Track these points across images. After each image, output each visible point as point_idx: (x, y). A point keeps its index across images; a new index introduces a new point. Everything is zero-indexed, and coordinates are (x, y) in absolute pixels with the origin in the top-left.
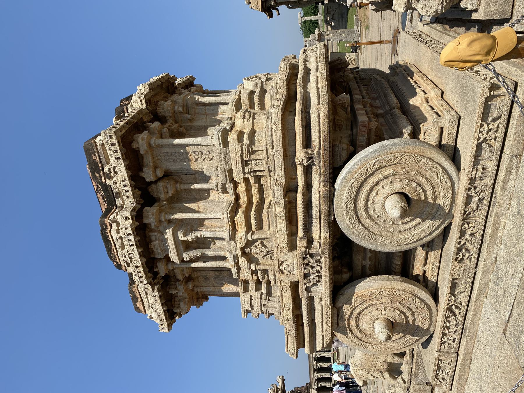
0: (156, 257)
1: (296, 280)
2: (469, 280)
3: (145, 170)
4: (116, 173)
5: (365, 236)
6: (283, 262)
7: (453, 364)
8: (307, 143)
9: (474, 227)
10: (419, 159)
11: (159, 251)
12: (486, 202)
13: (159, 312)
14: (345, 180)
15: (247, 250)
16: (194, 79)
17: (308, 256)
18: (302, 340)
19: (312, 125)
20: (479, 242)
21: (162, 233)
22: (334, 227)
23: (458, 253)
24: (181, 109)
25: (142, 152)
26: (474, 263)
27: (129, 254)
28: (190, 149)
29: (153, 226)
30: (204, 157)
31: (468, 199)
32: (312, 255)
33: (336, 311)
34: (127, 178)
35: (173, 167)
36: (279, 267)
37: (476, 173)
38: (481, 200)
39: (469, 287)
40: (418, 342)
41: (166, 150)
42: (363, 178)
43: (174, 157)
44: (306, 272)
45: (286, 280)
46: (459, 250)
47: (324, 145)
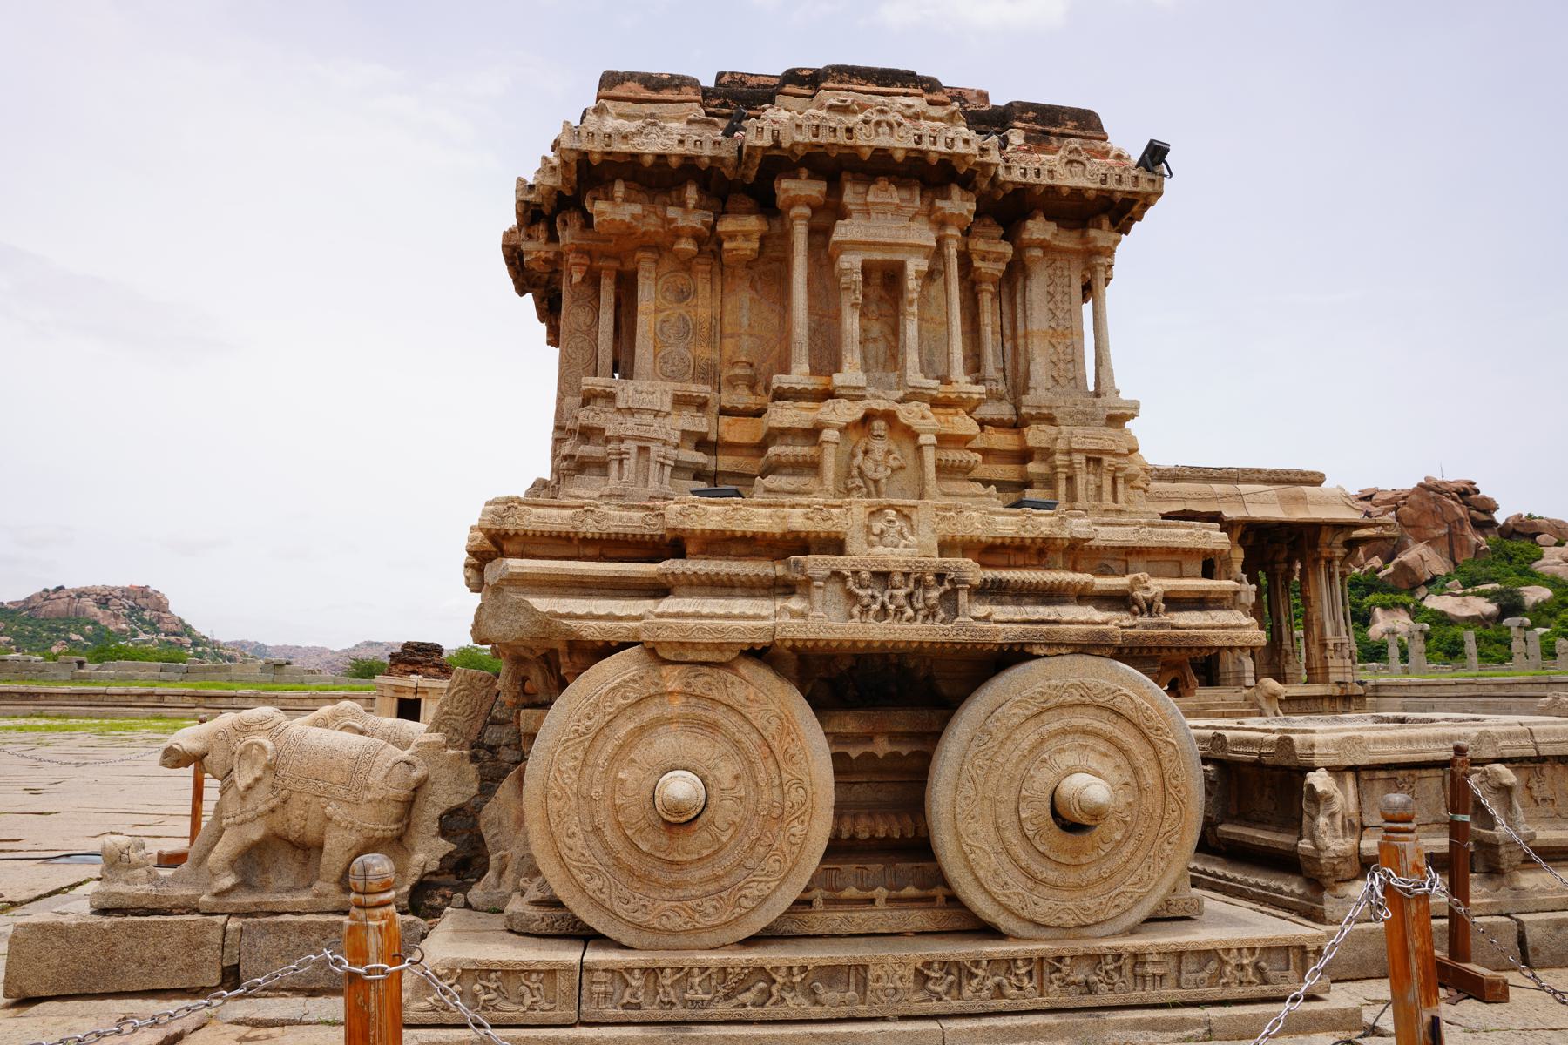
2: (862, 1010)
4: (1070, 162)
5: (990, 733)
6: (907, 517)
7: (537, 1015)
8: (1175, 602)
9: (1020, 988)
10: (1173, 839)
11: (870, 198)
12: (1089, 1001)
13: (636, 140)
14: (1135, 685)
15: (879, 426)
17: (947, 586)
18: (539, 552)
20: (981, 1010)
22: (1011, 656)
26: (918, 1009)
27: (890, 125)
29: (939, 203)
30: (1062, 366)
33: (729, 656)
36: (890, 506)
37: (1154, 963)
38: (1089, 988)
39: (843, 1011)
42: (1142, 719)
43: (1058, 297)
44: (897, 578)
45: (849, 518)
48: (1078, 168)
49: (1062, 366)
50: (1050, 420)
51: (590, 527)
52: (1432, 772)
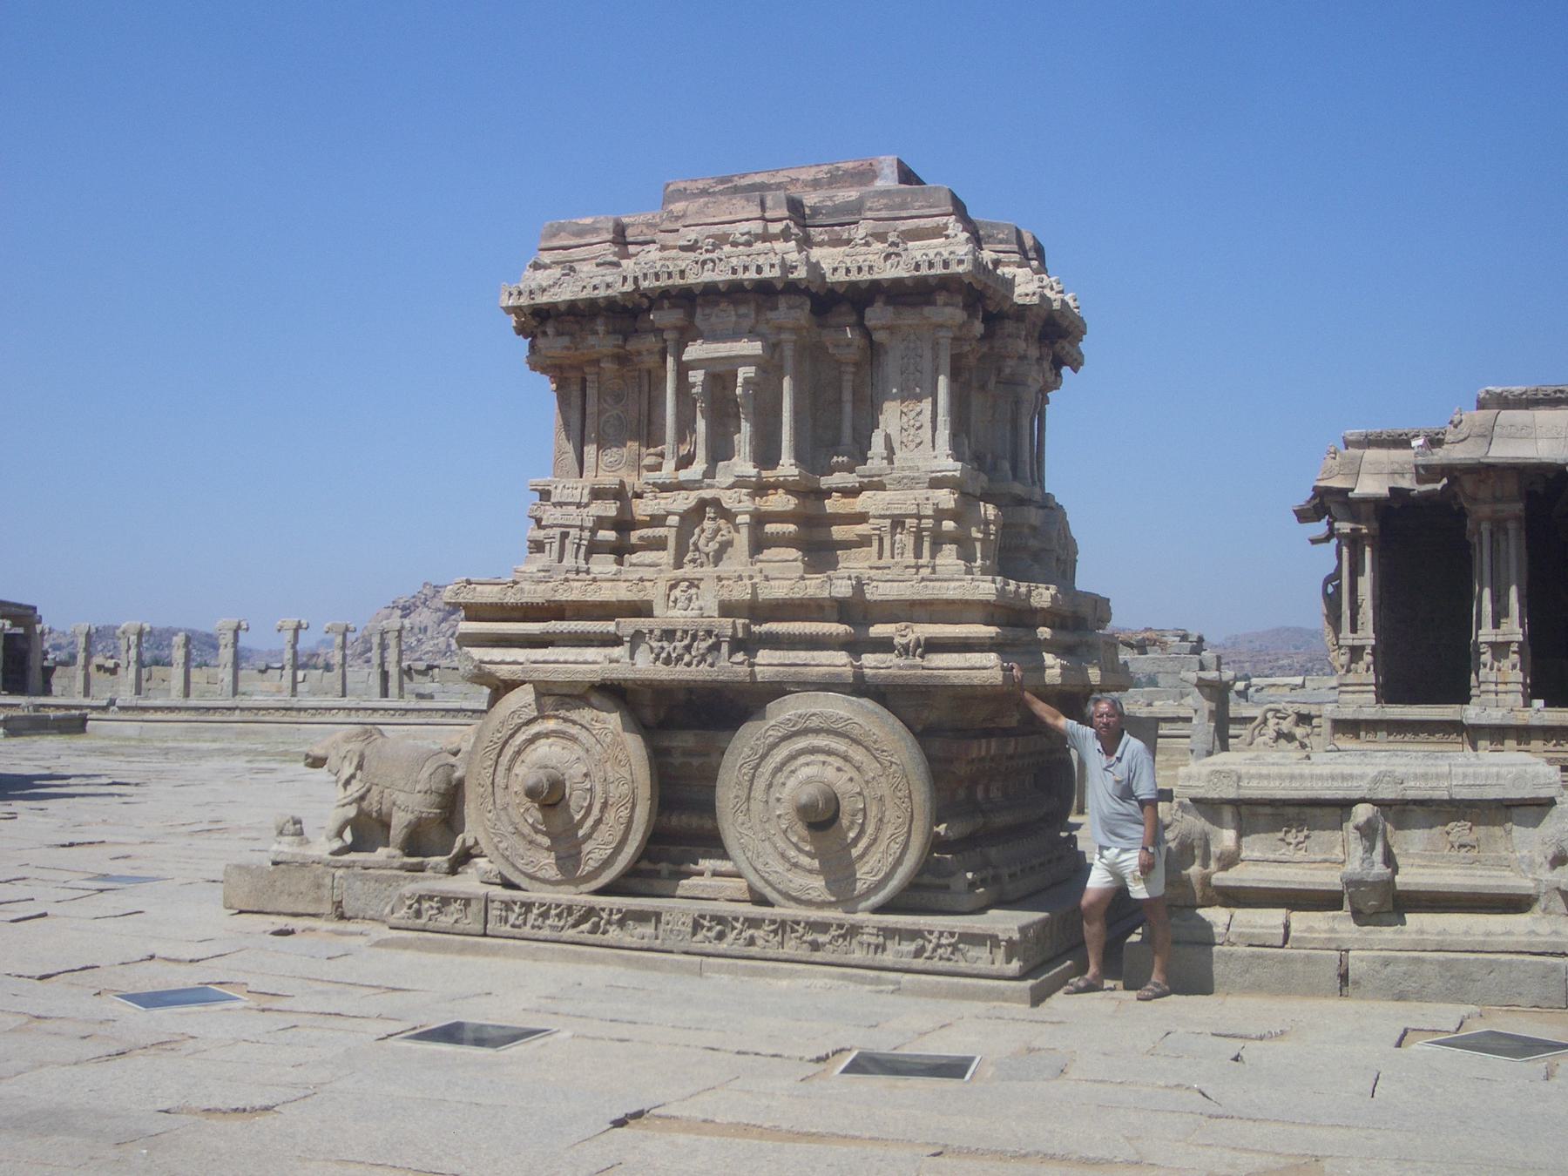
0: (699, 310)
1: (656, 613)
2: (657, 944)
3: (890, 308)
4: (888, 257)
8: (934, 646)
12: (818, 956)
13: (555, 290)
15: (710, 512)
16: (1075, 370)
19: (968, 655)
21: (753, 334)
23: (713, 918)
24: (1008, 371)
25: (927, 310)
28: (926, 405)
31: (823, 927)
32: (716, 647)
34: (876, 276)
35: (892, 365)
36: (685, 580)
39: (645, 943)
40: (502, 860)
41: (928, 354)
44: (679, 634)
46: (720, 920)
47: (931, 676)
48: (894, 259)
49: (912, 431)
50: (881, 487)
51: (511, 598)
52: (1328, 810)
